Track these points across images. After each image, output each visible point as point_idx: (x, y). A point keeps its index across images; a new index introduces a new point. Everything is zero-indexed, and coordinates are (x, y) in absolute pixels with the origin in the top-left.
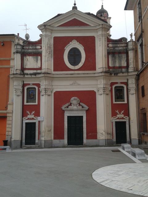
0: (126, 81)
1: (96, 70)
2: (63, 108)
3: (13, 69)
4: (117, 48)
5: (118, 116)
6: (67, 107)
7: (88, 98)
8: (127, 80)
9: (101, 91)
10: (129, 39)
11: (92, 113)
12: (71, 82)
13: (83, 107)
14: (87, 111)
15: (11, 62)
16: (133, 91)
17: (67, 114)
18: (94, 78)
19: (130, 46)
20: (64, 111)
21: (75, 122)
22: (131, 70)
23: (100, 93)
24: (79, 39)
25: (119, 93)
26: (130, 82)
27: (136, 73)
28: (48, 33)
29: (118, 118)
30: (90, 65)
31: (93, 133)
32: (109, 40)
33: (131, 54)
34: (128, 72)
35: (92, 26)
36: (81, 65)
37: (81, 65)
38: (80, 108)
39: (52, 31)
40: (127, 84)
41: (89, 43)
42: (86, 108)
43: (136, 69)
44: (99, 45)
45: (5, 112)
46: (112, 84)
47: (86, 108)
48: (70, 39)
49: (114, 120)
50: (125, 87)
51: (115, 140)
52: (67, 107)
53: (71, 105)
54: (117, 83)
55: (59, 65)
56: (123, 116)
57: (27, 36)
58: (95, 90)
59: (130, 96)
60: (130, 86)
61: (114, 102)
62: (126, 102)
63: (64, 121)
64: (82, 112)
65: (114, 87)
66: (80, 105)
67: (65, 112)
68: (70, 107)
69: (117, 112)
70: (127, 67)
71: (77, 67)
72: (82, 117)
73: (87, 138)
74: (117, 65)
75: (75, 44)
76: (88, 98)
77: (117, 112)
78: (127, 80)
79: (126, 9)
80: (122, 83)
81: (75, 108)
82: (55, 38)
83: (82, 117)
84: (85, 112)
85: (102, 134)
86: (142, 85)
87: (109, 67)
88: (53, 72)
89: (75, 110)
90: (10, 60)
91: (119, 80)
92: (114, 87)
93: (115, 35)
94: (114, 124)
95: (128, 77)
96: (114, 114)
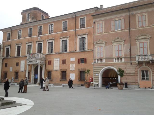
27: (3, 58)
33: (2, 50)
43: (3, 56)
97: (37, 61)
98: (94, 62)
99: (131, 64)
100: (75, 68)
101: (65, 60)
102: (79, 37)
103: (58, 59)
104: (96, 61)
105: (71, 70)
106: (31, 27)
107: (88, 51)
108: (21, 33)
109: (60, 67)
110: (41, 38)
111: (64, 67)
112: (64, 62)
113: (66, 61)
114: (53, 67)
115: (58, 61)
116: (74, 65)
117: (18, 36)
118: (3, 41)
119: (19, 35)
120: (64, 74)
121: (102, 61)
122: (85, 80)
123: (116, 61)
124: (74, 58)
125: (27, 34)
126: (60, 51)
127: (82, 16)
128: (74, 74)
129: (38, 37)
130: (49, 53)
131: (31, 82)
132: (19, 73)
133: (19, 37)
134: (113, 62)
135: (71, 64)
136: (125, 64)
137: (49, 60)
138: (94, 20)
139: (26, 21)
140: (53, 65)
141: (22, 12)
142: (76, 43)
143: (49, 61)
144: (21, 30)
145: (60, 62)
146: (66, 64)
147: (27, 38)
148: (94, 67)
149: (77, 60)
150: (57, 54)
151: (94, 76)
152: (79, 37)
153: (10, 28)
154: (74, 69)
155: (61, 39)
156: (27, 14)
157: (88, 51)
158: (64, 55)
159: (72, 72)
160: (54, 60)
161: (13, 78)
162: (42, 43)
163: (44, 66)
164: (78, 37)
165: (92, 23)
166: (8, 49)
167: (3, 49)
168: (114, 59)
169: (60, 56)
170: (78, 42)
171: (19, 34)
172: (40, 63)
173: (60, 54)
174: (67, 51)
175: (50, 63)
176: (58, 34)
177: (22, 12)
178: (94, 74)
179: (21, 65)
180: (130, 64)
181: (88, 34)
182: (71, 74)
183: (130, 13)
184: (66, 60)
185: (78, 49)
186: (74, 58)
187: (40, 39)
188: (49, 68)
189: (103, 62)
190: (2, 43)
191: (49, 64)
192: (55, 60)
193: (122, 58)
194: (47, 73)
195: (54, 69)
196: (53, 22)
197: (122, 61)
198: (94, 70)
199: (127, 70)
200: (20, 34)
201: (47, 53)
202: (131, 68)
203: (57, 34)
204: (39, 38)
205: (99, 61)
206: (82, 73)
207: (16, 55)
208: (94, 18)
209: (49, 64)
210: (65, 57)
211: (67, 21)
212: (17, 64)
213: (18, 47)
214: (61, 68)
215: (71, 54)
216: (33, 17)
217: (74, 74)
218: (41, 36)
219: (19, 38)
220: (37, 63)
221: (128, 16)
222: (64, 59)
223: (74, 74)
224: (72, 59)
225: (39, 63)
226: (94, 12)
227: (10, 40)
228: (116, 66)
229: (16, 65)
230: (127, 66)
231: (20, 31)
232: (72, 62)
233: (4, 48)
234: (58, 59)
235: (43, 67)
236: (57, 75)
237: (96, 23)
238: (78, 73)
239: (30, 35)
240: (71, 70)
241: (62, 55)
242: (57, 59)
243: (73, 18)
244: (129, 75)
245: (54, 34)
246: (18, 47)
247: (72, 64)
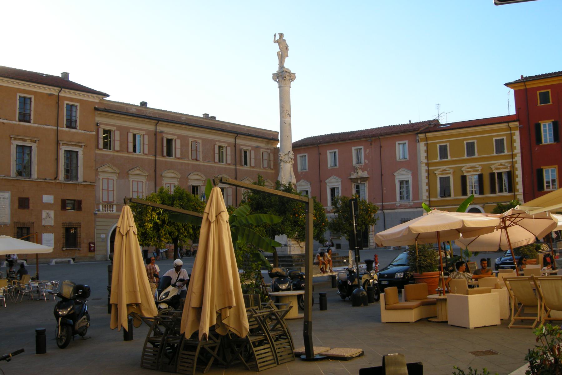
101: (28, 199)
105: (44, 226)
109: (12, 215)
113: (31, 201)
116: (52, 213)
124: (52, 197)
127: (72, 100)
135: (43, 211)
145: (12, 202)
148: (97, 219)
149: (60, 202)
154: (52, 223)
157: (85, 186)
159: (47, 229)
174: (33, 177)
176: (3, 123)
184: (30, 199)
186: (52, 197)
211: (33, 97)
222: (24, 196)
223: (52, 236)
224: (48, 199)
232: (48, 206)
234: (7, 195)
238: (62, 231)
240: (43, 224)
247: (47, 211)
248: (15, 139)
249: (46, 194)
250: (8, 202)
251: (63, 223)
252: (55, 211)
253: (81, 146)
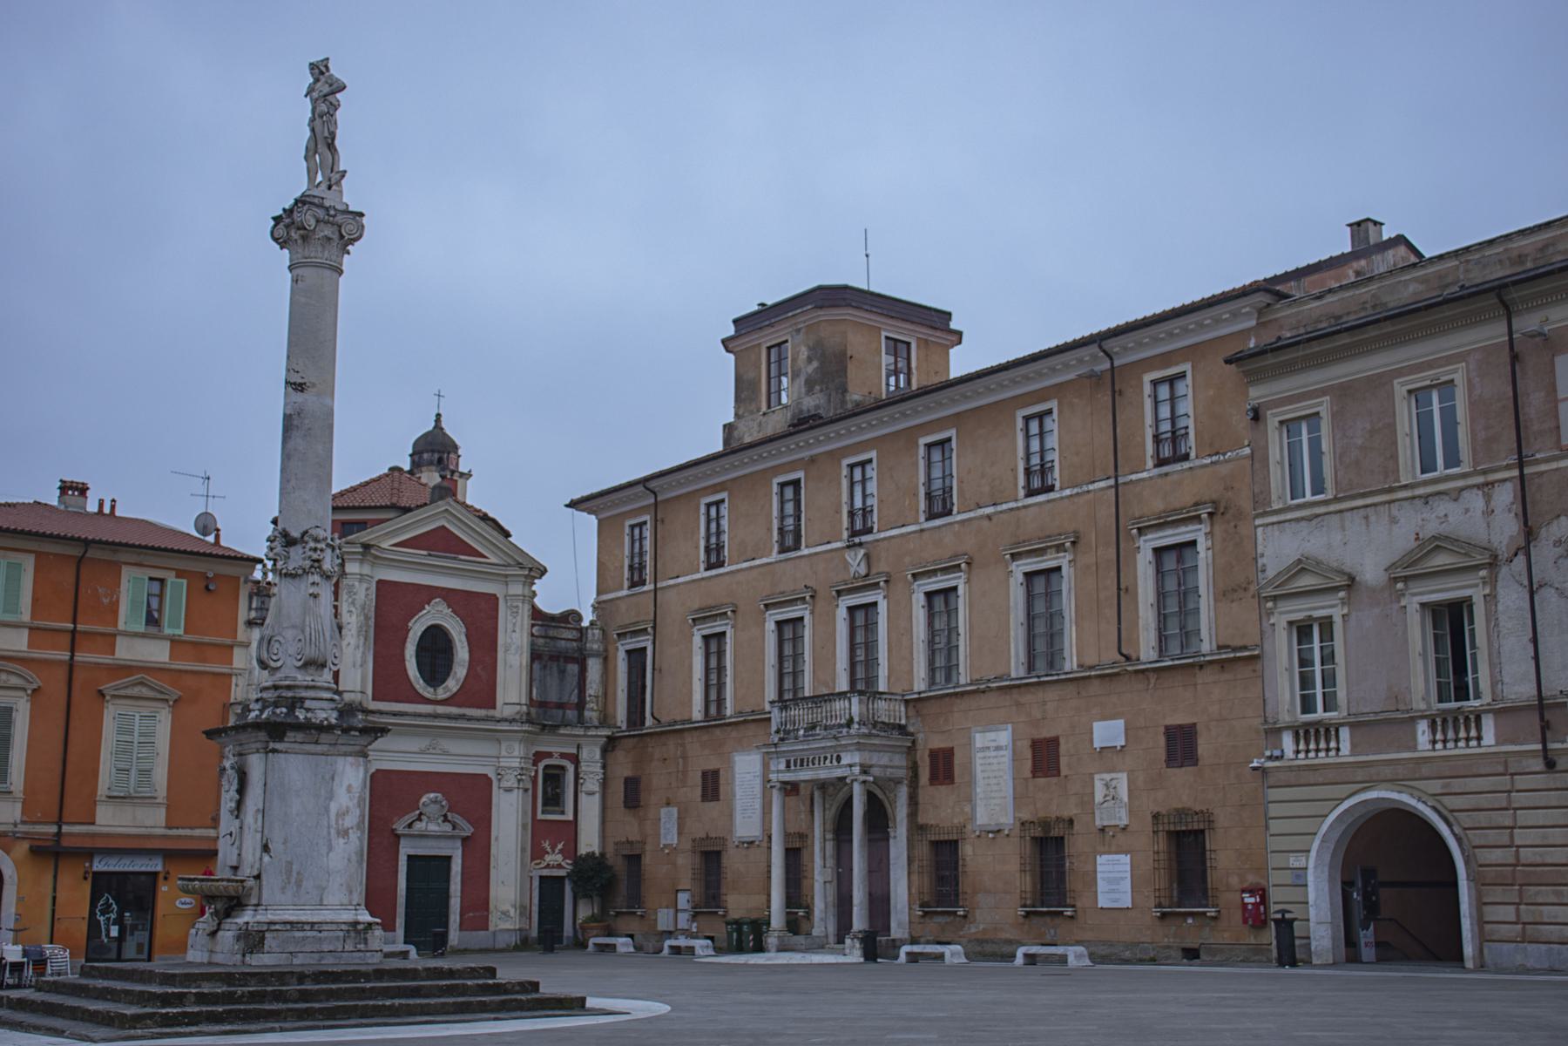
0: (574, 751)
1: (494, 707)
2: (400, 827)
3: (242, 681)
4: (558, 643)
5: (548, 858)
6: (410, 826)
7: (470, 797)
8: (579, 747)
9: (510, 781)
10: (588, 617)
11: (478, 848)
12: (423, 743)
13: (454, 828)
14: (465, 840)
15: (238, 653)
16: (592, 784)
17: (406, 849)
18: (494, 736)
19: (594, 645)
20: (398, 837)
21: (429, 871)
22: (591, 714)
23: (505, 784)
24: (451, 597)
25: (551, 785)
26: (584, 755)
27: (607, 732)
28: (366, 570)
29: (548, 866)
30: (481, 691)
31: (478, 909)
32: (537, 614)
33: (594, 668)
34: (581, 721)
35: (493, 560)
36: (452, 685)
37: (452, 685)
38: (448, 827)
39: (378, 561)
40: (575, 760)
41: (480, 614)
42: (468, 830)
44: (510, 626)
45: (212, 833)
46: (539, 756)
47: (468, 830)
48: (431, 593)
49: (536, 874)
50: (571, 768)
51: (534, 933)
52: (410, 826)
53: (419, 819)
54: (550, 755)
55: (388, 681)
56: (559, 858)
57: (206, 524)
58: (492, 775)
59: (583, 798)
60: (583, 767)
61: (540, 816)
62: (570, 817)
63: (396, 872)
64: (449, 843)
65: (541, 766)
66: (446, 819)
67: (403, 842)
68: (418, 826)
69: (546, 845)
70: (581, 705)
71: (442, 694)
72: (449, 858)
73: (462, 927)
74: (553, 697)
75: (436, 614)
76: (470, 797)
77: (546, 845)
78: (579, 747)
79: (573, 504)
80: (563, 756)
81: (433, 827)
82: (380, 582)
83: (449, 858)
84: (459, 843)
85: (505, 913)
86: (628, 773)
87: (531, 702)
88: (374, 706)
89: (430, 831)
90: (231, 647)
91: (555, 746)
92: (541, 766)
93: (551, 597)
94: (536, 883)
95: (581, 741)
96: (537, 853)
97: (839, 759)
98: (1268, 753)
99: (1550, 765)
100: (1131, 812)
101: (1054, 742)
102: (1147, 545)
103: (1004, 737)
104: (1288, 741)
105: (1103, 830)
106: (792, 466)
107: (1223, 665)
108: (725, 523)
109: (1018, 799)
110: (867, 556)
111: (1052, 802)
112: (1044, 757)
113: (1063, 748)
114: (970, 799)
115: (998, 748)
117: (708, 550)
118: (599, 593)
119: (713, 540)
120: (1050, 853)
121: (1473, 733)
122: (1211, 912)
123: (1434, 742)
124: (1120, 723)
125: (770, 530)
126: (1017, 669)
127: (1166, 359)
128: (1126, 859)
129: (849, 556)
130: (932, 682)
131: (815, 932)
132: (725, 861)
133: (715, 557)
134: (1414, 748)
135: (1097, 777)
136: (1505, 766)
137: (938, 743)
138: (1257, 394)
139: (764, 408)
140: (971, 783)
141: (731, 331)
142: (1124, 591)
143: (934, 755)
144: (724, 495)
145: (1016, 758)
146: (1064, 771)
147: (765, 560)
148: (1274, 794)
150: (991, 689)
151: (1275, 878)
152: (1147, 545)
153: (644, 481)
155: (1013, 567)
156: (769, 348)
157: (1223, 665)
158: (1044, 703)
159: (1107, 838)
160: (969, 743)
161: (683, 900)
162: (875, 604)
163: (903, 792)
164: (1141, 542)
165: (1241, 421)
166: (636, 656)
167: (606, 659)
168: (1423, 726)
169: (1018, 704)
170: (1140, 583)
171: (713, 526)
172: (865, 772)
173: (1015, 694)
175: (944, 767)
176: (989, 517)
177: (731, 331)
178: (1274, 861)
179: (739, 793)
180: (1538, 764)
181: (1210, 514)
182: (1105, 857)
183: (1514, 321)
184: (1062, 741)
185: (1147, 649)
186: (1120, 723)
187: (863, 565)
188: (940, 808)
189: (1338, 749)
190: (598, 607)
191: (934, 779)
192: (980, 740)
193: (1478, 719)
194: (924, 850)
195: (973, 818)
196: (957, 419)
197: (1479, 738)
198: (1275, 826)
199: (1524, 817)
200: (719, 533)
201: (920, 684)
202: (1553, 798)
203: (981, 517)
204: (856, 562)
205: (1307, 743)
206: (1184, 853)
207: (697, 713)
208: (1255, 377)
209: (934, 779)
210: (1054, 713)
212: (712, 786)
213: (706, 638)
214: (1026, 816)
215: (1095, 688)
216: (810, 369)
217: (1126, 859)
218: (864, 538)
219: (709, 567)
220: (839, 773)
221: (1505, 357)
222: (1046, 733)
224: (1108, 732)
225: (857, 770)
226: (1253, 323)
227: (649, 587)
228: (1435, 786)
229: (699, 791)
230: (1521, 782)
231: (718, 503)
233: (606, 650)
234: (1004, 737)
235: (893, 803)
236: (997, 875)
237: (1272, 421)
239: (790, 540)
240: (1098, 823)
241: (1027, 698)
242: (992, 735)
243: (1094, 378)
244: (1538, 860)
245: (963, 522)
246: (706, 638)
247: (1108, 777)
248: (1014, 557)
249: (1104, 718)
250: (1006, 757)
251: (1156, 816)
252: (1131, 773)
253: (1197, 519)
